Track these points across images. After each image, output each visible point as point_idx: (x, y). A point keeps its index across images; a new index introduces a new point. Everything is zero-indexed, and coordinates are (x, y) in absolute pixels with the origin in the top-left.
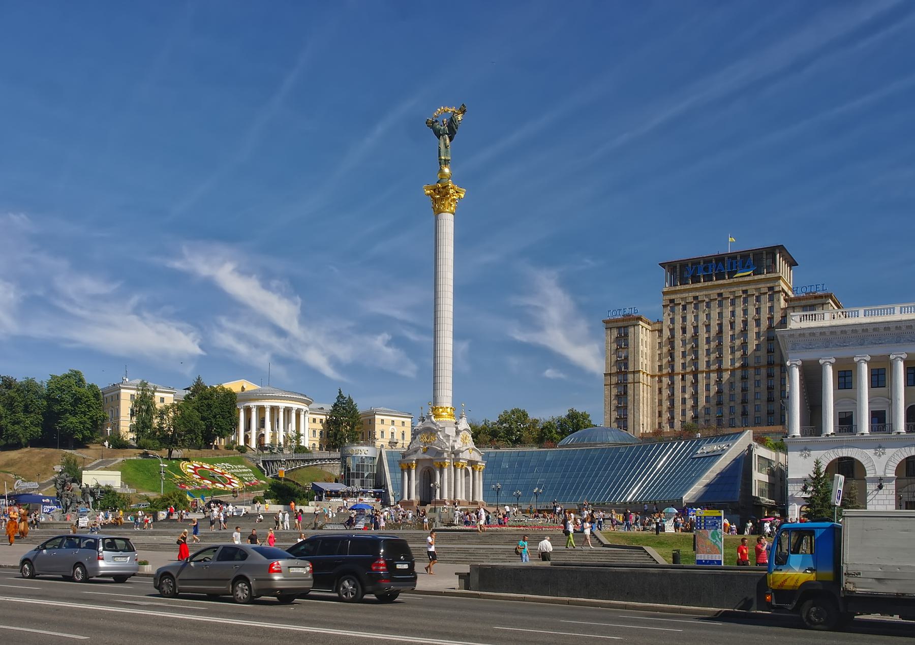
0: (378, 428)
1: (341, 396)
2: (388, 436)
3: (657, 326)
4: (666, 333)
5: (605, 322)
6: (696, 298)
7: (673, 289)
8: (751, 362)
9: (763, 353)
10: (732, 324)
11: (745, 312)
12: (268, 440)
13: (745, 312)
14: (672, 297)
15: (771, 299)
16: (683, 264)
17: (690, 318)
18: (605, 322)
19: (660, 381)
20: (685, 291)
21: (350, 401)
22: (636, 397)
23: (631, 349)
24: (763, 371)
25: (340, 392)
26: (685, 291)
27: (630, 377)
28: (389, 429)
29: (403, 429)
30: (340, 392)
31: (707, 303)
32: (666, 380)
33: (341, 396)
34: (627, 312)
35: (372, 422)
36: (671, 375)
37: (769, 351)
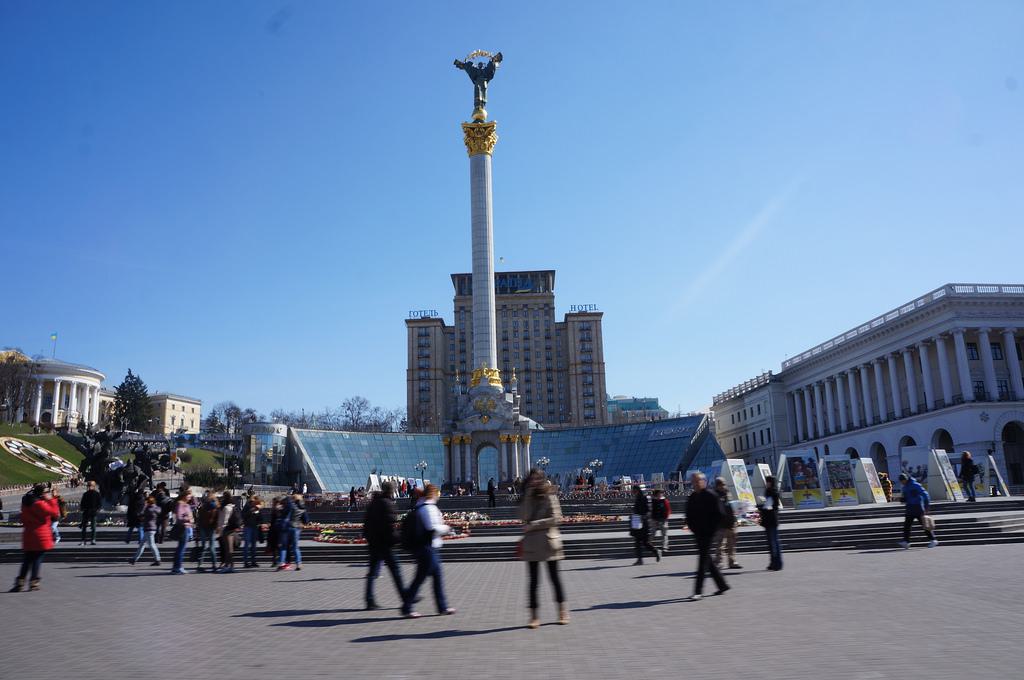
1: (130, 376)
4: (457, 336)
5: (407, 321)
7: (462, 297)
8: (533, 365)
9: (542, 359)
10: (515, 332)
11: (527, 323)
12: (57, 421)
13: (527, 323)
18: (407, 321)
21: (138, 382)
24: (544, 375)
25: (130, 372)
28: (179, 415)
29: (192, 416)
30: (130, 372)
33: (130, 376)
34: (428, 313)
37: (548, 359)
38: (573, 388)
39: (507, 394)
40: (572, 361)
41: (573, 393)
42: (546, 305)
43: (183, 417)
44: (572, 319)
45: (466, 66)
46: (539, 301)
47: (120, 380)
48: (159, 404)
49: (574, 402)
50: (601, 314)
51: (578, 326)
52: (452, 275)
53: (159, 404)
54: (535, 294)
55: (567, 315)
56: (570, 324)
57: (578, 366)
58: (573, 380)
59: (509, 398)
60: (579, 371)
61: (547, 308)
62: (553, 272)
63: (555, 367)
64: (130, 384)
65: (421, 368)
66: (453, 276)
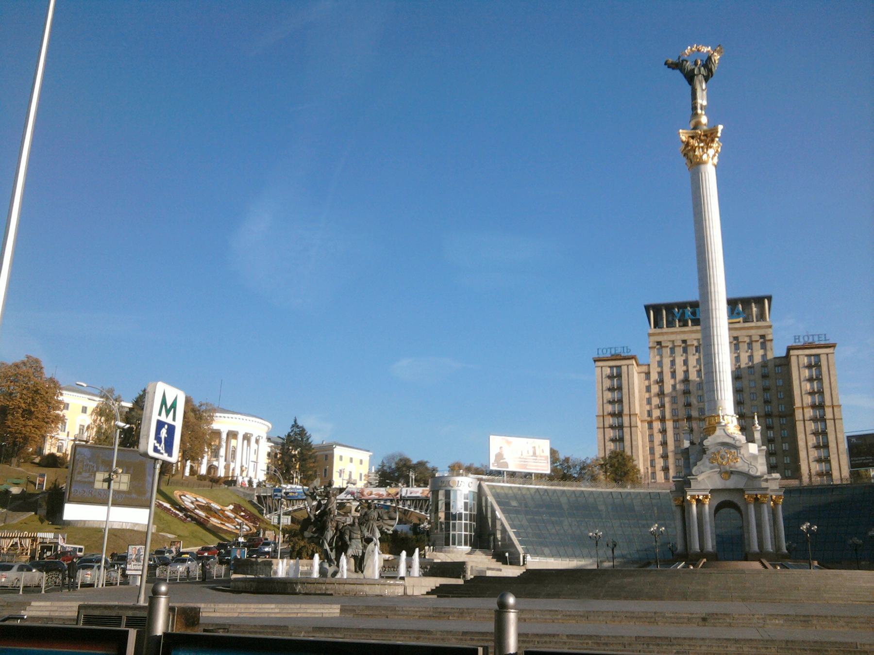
0: (337, 465)
1: (295, 425)
2: (346, 476)
3: (645, 369)
6: (684, 341)
14: (659, 339)
15: (764, 346)
16: (669, 307)
17: (679, 360)
19: (651, 427)
20: (672, 333)
21: (302, 432)
22: (634, 443)
23: (625, 390)
26: (672, 333)
27: (626, 420)
31: (671, 349)
32: (657, 425)
33: (295, 425)
35: (328, 458)
36: (662, 419)
38: (801, 436)
39: (750, 444)
40: (798, 403)
41: (801, 444)
42: (762, 336)
43: (352, 469)
44: (792, 352)
45: (677, 66)
46: (752, 332)
47: (284, 431)
48: (326, 456)
49: (803, 454)
50: (833, 346)
51: (806, 360)
52: (647, 308)
53: (326, 456)
54: (747, 325)
55: (789, 349)
56: (793, 360)
57: (805, 410)
58: (800, 426)
59: (753, 448)
60: (807, 416)
61: (762, 340)
62: (770, 298)
63: (775, 412)
64: (296, 434)
65: (613, 415)
66: (647, 308)
